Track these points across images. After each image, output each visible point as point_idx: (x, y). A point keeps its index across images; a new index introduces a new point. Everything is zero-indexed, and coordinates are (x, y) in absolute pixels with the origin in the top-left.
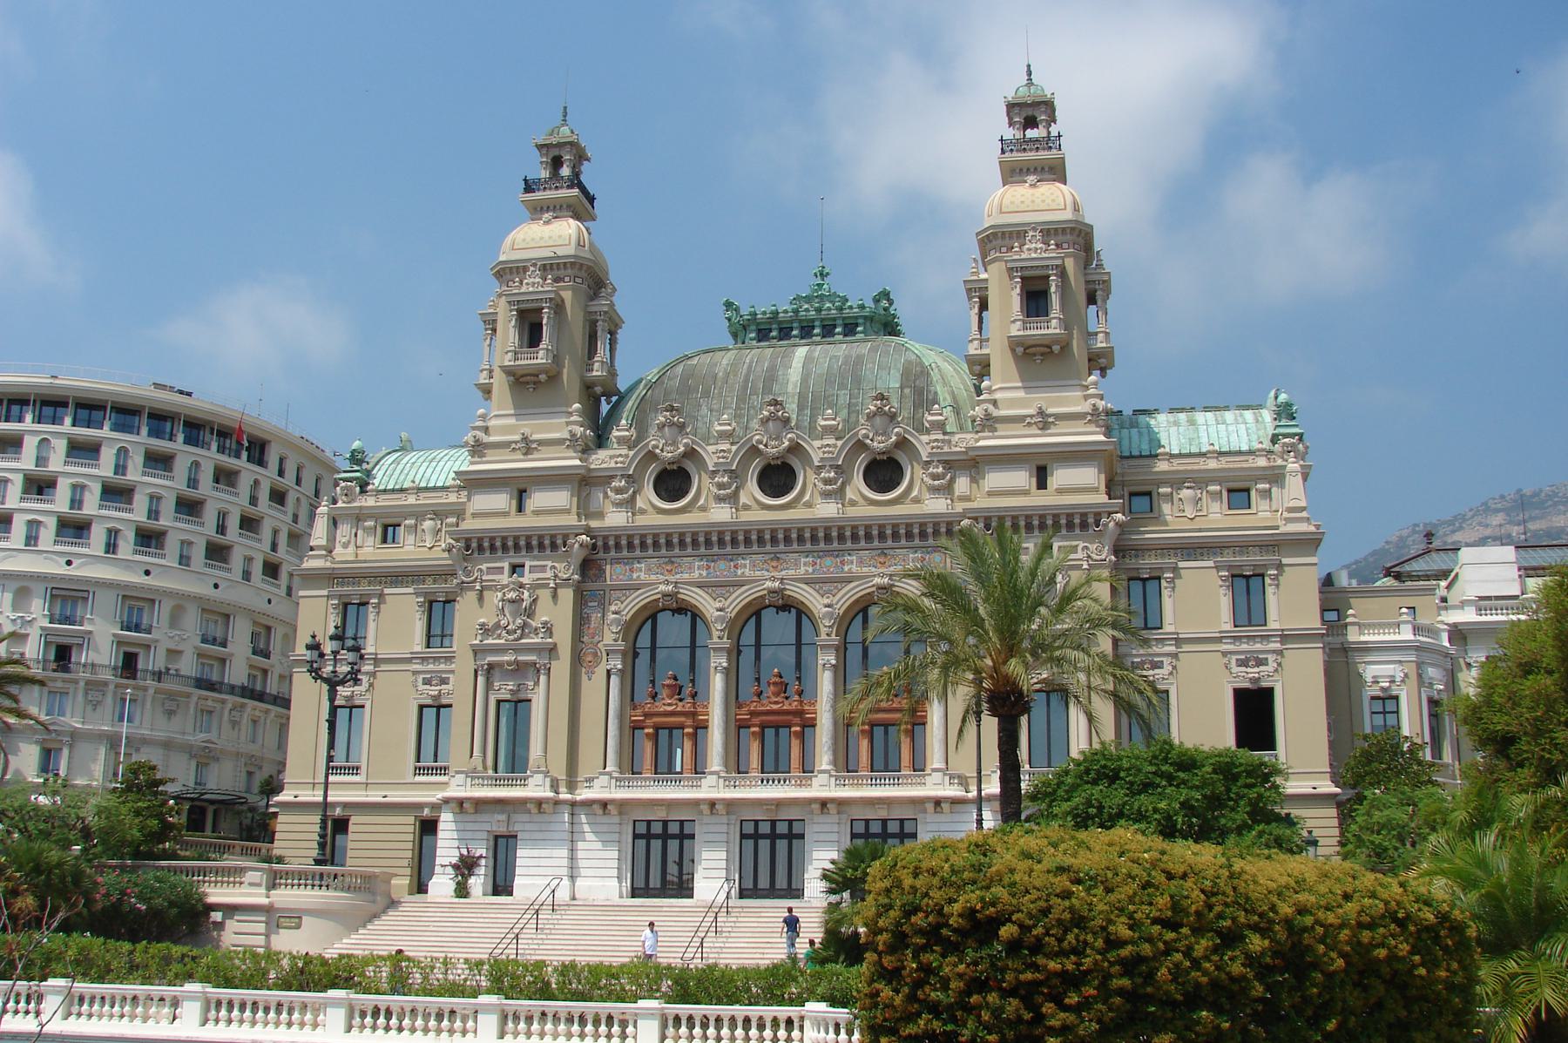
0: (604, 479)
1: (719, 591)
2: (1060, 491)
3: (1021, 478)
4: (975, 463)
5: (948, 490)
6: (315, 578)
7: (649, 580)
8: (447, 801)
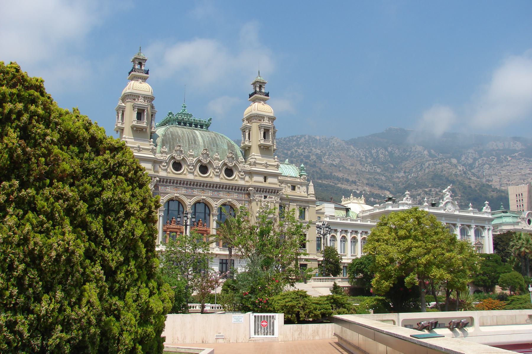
0: (161, 162)
1: (189, 197)
2: (269, 183)
3: (261, 179)
4: (251, 174)
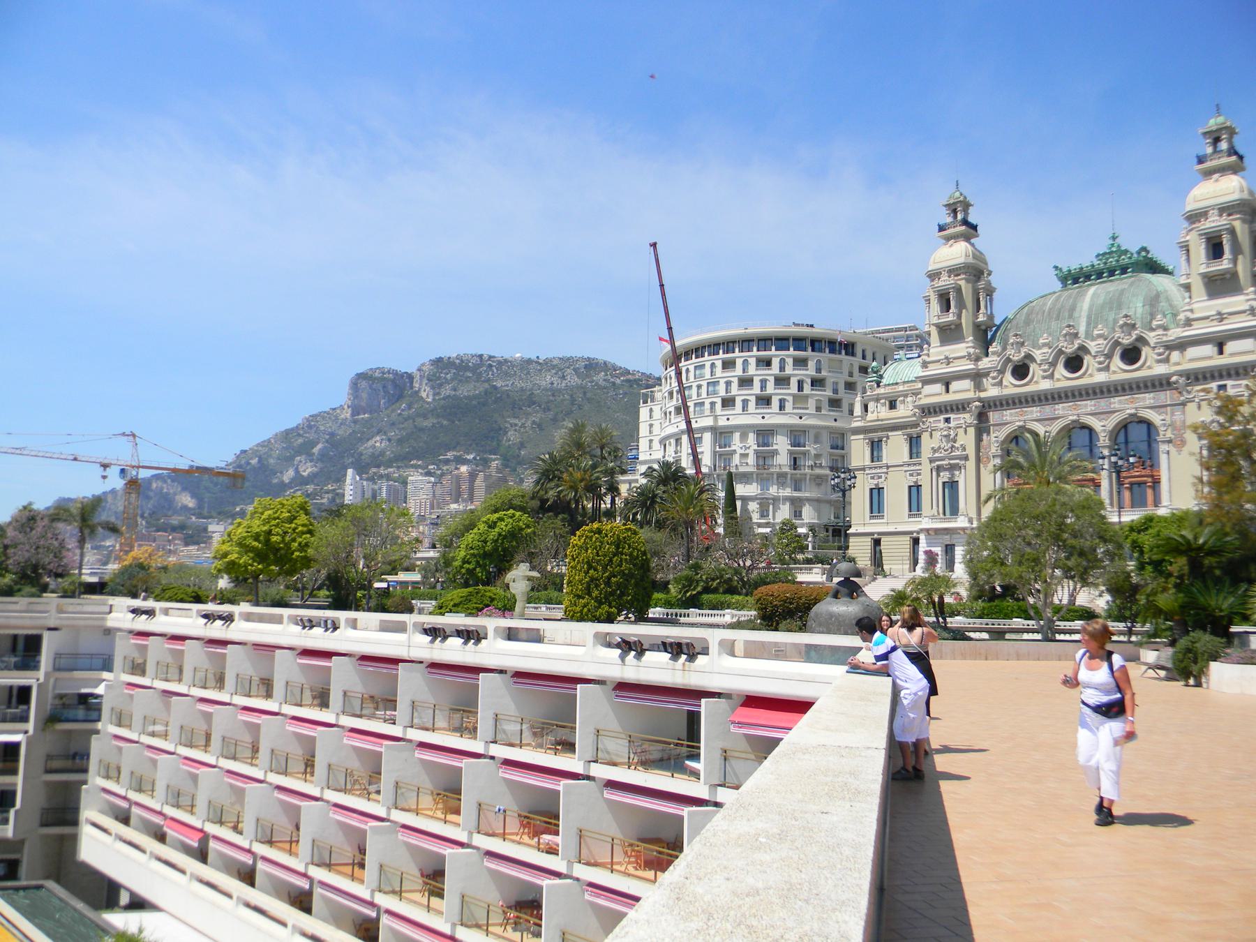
2: (1232, 355)
3: (1209, 350)
4: (1182, 345)
5: (1167, 360)
6: (857, 431)
7: (1011, 419)
8: (922, 530)
